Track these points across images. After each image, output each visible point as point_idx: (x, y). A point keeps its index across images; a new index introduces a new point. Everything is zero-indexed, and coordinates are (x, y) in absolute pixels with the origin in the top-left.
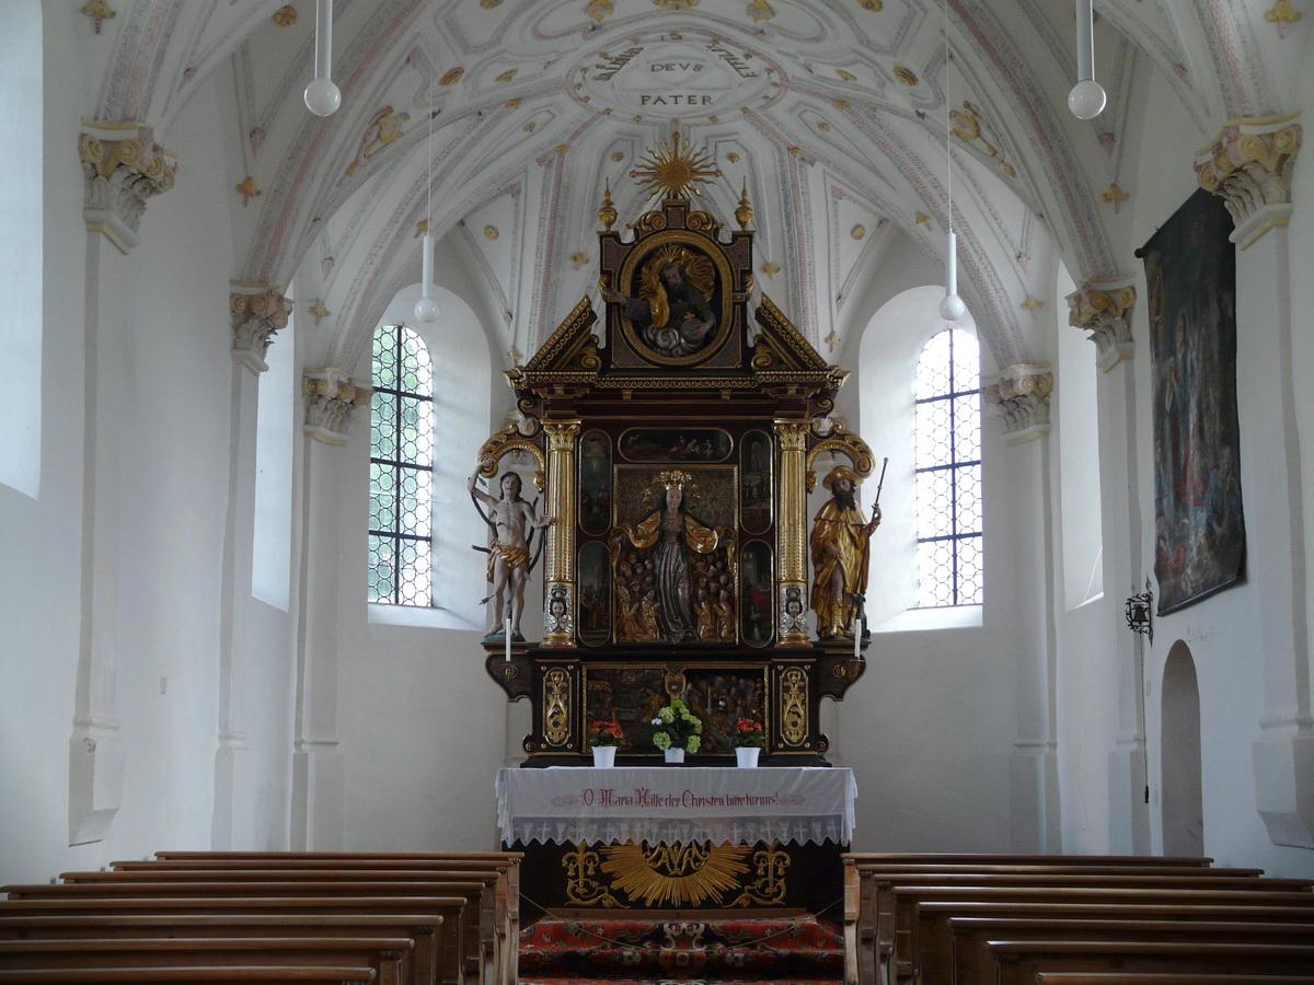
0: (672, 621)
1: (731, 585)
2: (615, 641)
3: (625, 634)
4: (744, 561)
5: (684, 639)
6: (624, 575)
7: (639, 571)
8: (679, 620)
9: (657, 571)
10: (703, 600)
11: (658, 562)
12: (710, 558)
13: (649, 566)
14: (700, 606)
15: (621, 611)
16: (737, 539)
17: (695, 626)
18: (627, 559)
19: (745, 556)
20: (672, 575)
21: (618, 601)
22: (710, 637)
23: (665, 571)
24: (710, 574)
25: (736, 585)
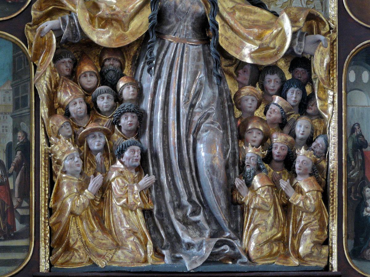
0: (185, 222)
1: (320, 141)
2: (44, 267)
3: (68, 248)
4: (351, 88)
5: (212, 259)
6: (67, 114)
7: (103, 103)
8: (200, 217)
9: (146, 105)
10: (259, 170)
11: (148, 82)
12: (272, 81)
13: (128, 93)
14: (249, 184)
15: (58, 196)
16: (335, 36)
17: (238, 232)
18: (73, 75)
19: (352, 77)
20: (184, 111)
21: (52, 174)
22: (271, 255)
23: (166, 103)
24: (274, 113)
25: (333, 140)
